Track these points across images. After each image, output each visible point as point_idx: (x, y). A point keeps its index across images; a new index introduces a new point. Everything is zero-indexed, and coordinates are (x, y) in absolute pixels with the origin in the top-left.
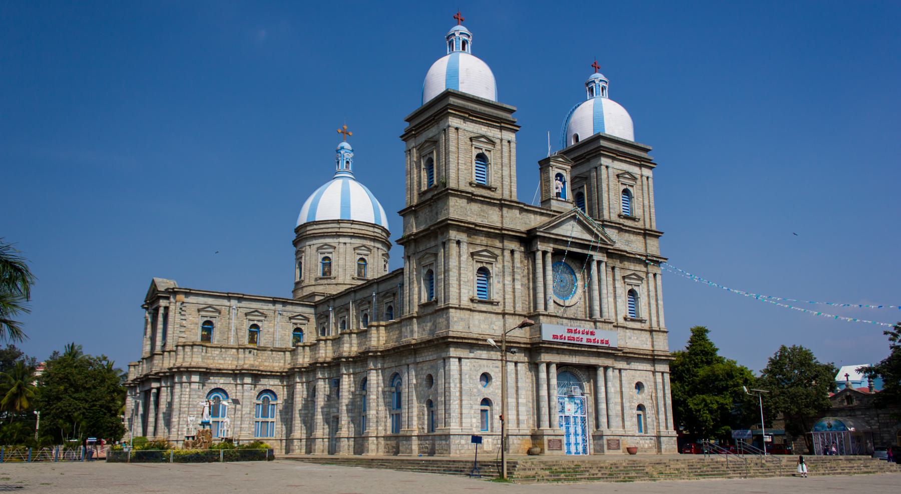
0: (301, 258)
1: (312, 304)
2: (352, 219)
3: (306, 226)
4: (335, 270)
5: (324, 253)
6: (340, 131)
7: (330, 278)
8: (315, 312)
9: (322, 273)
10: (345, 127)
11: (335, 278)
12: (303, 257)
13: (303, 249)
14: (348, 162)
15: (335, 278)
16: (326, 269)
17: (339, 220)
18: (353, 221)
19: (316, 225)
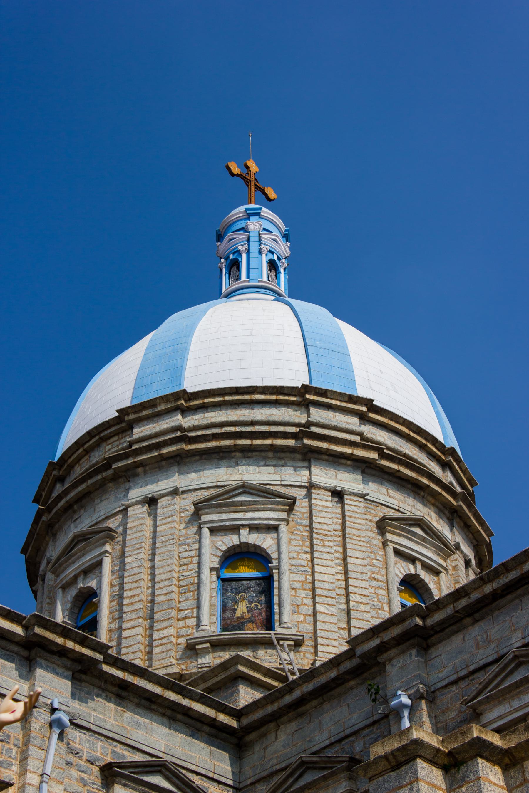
0: (99, 564)
1: (222, 718)
2: (362, 392)
3: (130, 427)
4: (296, 609)
5: (235, 529)
6: (236, 170)
7: (268, 644)
8: (237, 773)
9: (217, 620)
10: (254, 168)
11: (298, 644)
12: (107, 562)
13: (112, 524)
14: (273, 266)
15: (298, 644)
16: (242, 609)
17: (306, 389)
18: (369, 403)
19: (185, 411)
